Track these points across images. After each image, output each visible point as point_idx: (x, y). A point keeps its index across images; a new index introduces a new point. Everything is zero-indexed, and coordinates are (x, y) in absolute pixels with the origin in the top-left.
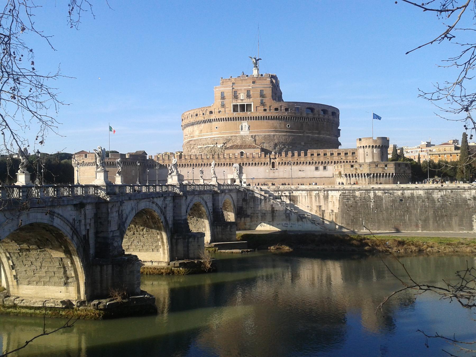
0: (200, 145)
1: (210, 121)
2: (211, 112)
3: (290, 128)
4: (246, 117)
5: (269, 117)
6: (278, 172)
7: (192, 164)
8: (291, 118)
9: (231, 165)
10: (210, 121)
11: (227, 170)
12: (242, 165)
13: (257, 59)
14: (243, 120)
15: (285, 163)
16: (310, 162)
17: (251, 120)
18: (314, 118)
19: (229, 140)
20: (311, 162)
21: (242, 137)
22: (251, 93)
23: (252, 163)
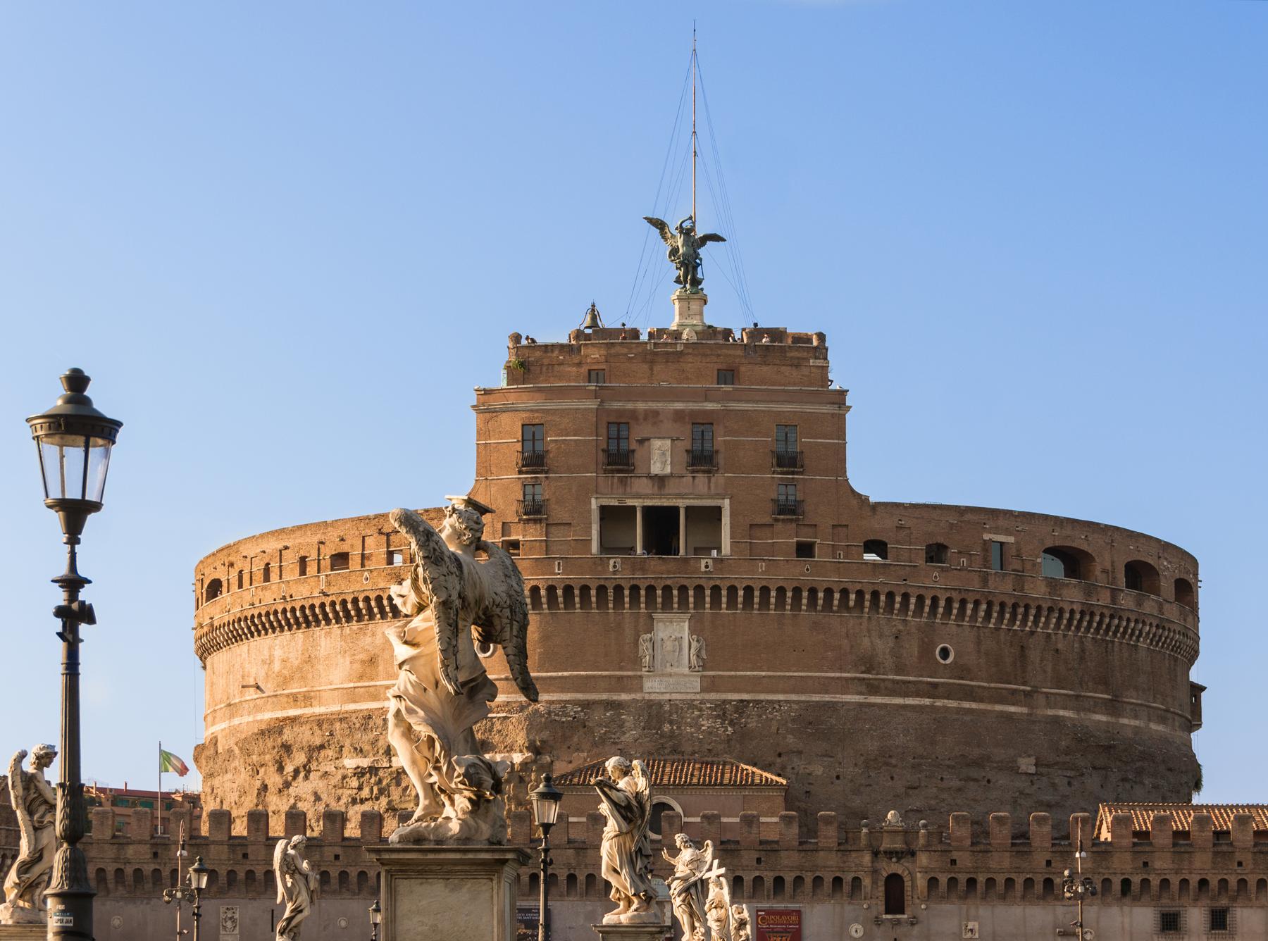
0: (360, 752)
3: (961, 670)
4: (683, 589)
5: (829, 592)
8: (963, 602)
13: (700, 233)
14: (667, 605)
16: (1126, 884)
18: (1087, 612)
21: (654, 713)
22: (720, 439)
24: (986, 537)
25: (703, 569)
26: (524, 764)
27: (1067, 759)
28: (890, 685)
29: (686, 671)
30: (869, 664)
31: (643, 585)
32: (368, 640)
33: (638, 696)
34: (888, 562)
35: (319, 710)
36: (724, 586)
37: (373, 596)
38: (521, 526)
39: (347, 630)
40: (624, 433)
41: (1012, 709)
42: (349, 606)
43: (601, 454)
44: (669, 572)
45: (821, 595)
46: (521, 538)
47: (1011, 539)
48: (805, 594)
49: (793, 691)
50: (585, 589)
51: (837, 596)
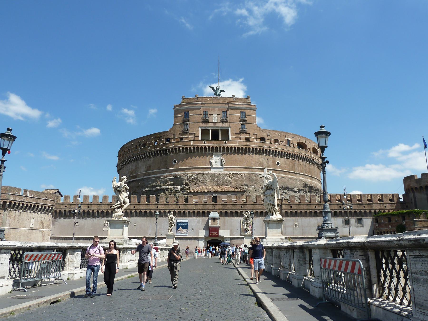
7: (138, 211)
9: (206, 214)
10: (165, 152)
13: (220, 90)
14: (216, 151)
15: (296, 212)
20: (338, 211)
21: (213, 176)
22: (228, 114)
24: (286, 138)
26: (183, 188)
27: (303, 189)
31: (211, 147)
32: (149, 162)
33: (210, 172)
34: (266, 142)
35: (138, 179)
36: (229, 147)
40: (207, 114)
47: (291, 139)
49: (245, 171)
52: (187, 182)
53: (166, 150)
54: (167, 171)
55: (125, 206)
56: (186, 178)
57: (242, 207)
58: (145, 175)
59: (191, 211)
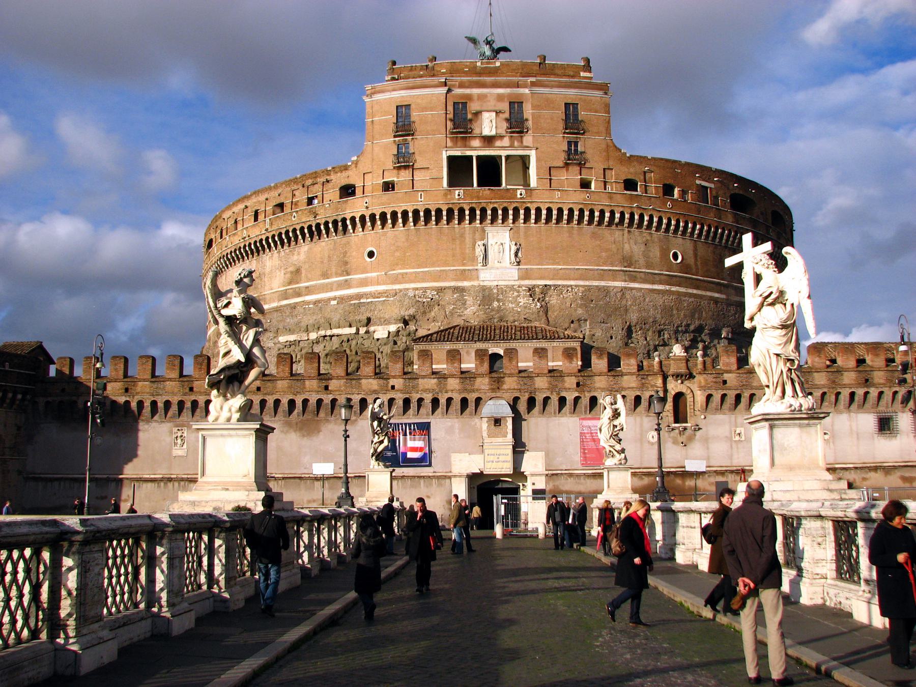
0: (291, 331)
1: (341, 226)
2: (348, 191)
3: (684, 267)
4: (505, 210)
5: (602, 212)
6: (706, 440)
9: (472, 405)
11: (450, 431)
12: (522, 406)
13: (495, 46)
15: (738, 398)
17: (527, 219)
19: (426, 307)
20: (860, 392)
21: (487, 296)
23: (577, 399)
24: (698, 182)
25: (519, 196)
28: (642, 275)
29: (508, 265)
30: (628, 261)
32: (295, 257)
33: (475, 283)
37: (298, 227)
38: (395, 171)
39: (283, 253)
41: (716, 295)
42: (284, 236)
43: (449, 123)
44: (495, 198)
45: (597, 214)
46: (395, 179)
47: (712, 186)
48: (587, 213)
50: (439, 211)
51: (607, 215)
52: (412, 311)
53: (344, 220)
54: (347, 284)
55: (253, 374)
56: (407, 301)
57: (578, 384)
58: (285, 295)
59: (428, 398)
